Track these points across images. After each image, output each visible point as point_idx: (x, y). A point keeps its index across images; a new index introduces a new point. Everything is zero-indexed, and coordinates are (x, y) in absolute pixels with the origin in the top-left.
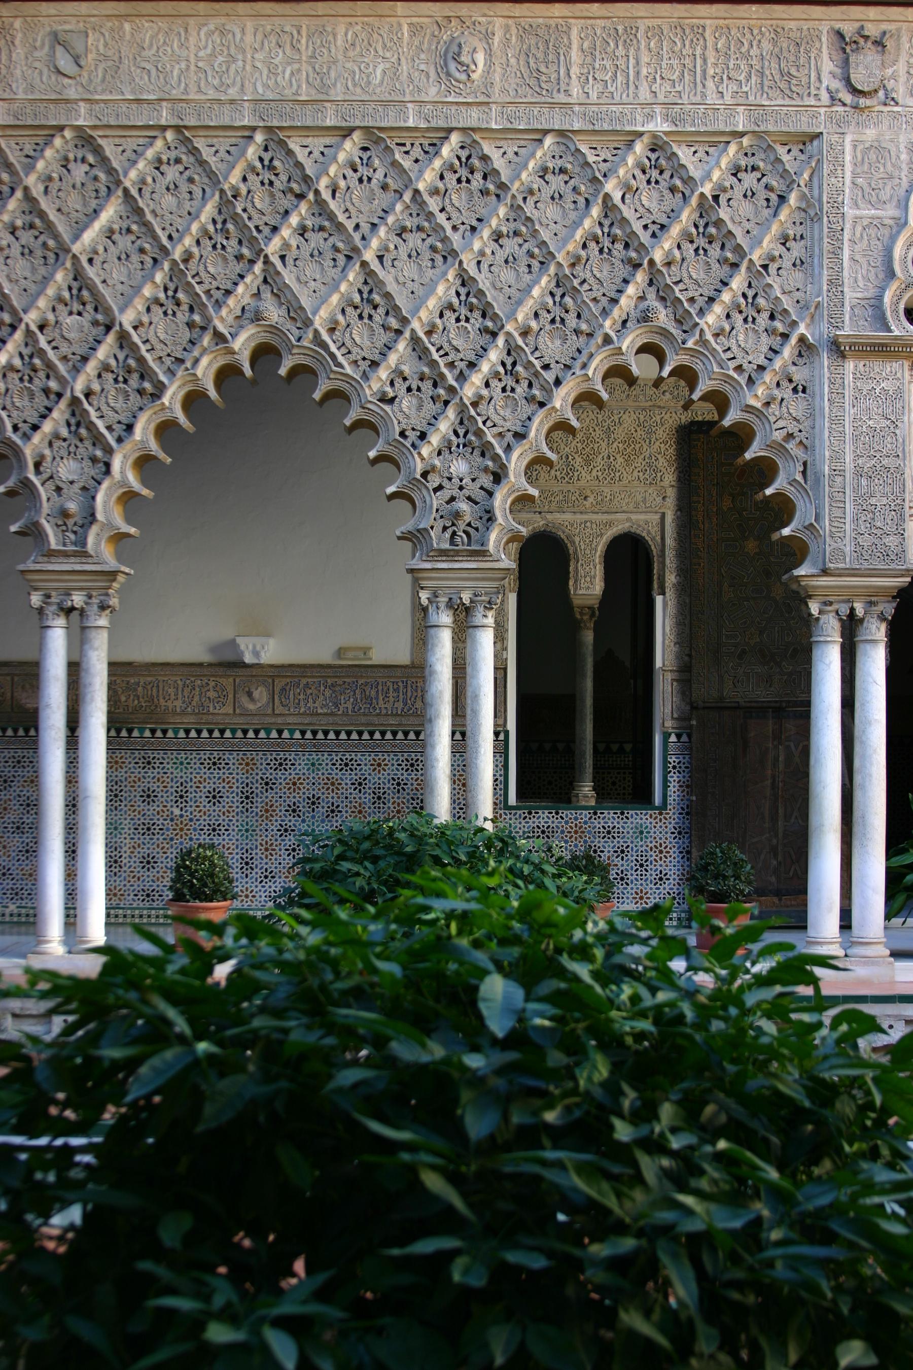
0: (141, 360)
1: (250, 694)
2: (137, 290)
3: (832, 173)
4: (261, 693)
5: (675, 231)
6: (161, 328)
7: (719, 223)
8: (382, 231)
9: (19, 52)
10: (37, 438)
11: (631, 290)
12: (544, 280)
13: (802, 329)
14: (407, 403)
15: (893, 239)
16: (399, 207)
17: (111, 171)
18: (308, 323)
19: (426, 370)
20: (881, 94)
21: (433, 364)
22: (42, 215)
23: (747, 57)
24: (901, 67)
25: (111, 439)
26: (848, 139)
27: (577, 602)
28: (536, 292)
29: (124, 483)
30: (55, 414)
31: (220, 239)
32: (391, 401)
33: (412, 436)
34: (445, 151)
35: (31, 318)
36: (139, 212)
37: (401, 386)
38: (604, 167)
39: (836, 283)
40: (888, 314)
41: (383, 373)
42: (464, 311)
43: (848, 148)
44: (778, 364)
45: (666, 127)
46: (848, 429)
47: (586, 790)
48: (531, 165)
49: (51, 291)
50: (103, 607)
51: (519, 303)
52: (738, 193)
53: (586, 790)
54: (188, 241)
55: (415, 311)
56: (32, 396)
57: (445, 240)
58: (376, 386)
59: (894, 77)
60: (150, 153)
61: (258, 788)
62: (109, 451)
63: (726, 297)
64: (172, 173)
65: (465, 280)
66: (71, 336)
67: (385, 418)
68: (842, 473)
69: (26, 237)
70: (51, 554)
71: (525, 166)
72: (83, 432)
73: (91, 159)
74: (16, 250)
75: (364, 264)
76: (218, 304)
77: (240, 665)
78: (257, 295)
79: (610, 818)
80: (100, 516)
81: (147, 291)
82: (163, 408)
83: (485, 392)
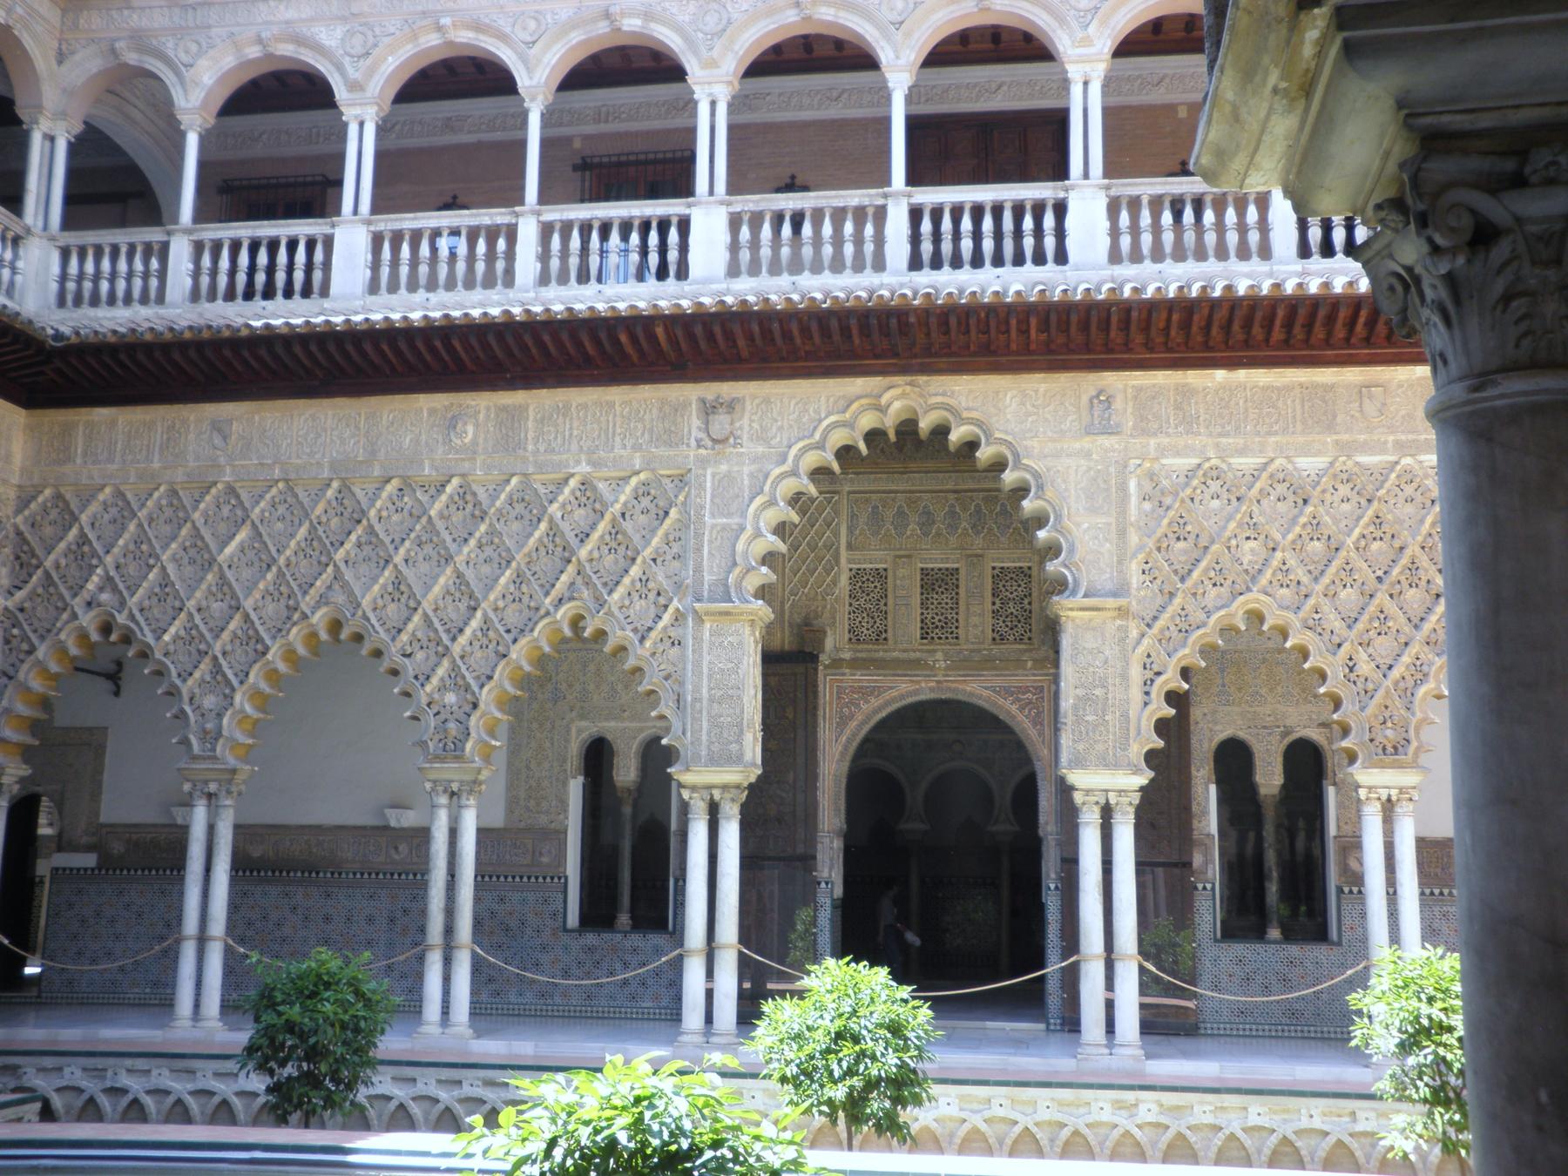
0: (256, 631)
1: (396, 848)
2: (256, 584)
3: (699, 495)
4: (403, 848)
5: (595, 536)
6: (270, 608)
7: (625, 534)
8: (407, 543)
9: (192, 436)
10: (190, 682)
11: (564, 578)
12: (508, 573)
13: (675, 603)
14: (420, 656)
15: (737, 538)
16: (418, 527)
17: (245, 509)
18: (359, 605)
19: (432, 635)
20: (731, 440)
21: (436, 631)
22: (202, 539)
23: (642, 420)
24: (746, 421)
25: (235, 682)
26: (709, 472)
27: (618, 784)
28: (503, 580)
29: (242, 711)
30: (202, 666)
31: (309, 551)
32: (409, 656)
33: (421, 678)
34: (449, 489)
35: (191, 605)
36: (260, 535)
37: (416, 645)
38: (551, 496)
39: (698, 569)
40: (732, 590)
41: (404, 637)
42: (458, 595)
43: (709, 478)
44: (661, 624)
45: (588, 469)
46: (705, 670)
47: (624, 919)
48: (503, 496)
49: (204, 586)
50: (229, 792)
51: (492, 588)
52: (638, 510)
53: (624, 919)
54: (288, 552)
55: (424, 596)
56: (190, 654)
57: (446, 548)
58: (399, 644)
59: (741, 428)
60: (268, 496)
61: (399, 914)
62: (233, 690)
63: (626, 580)
64: (281, 510)
65: (459, 575)
66: (217, 615)
67: (404, 667)
68: (700, 700)
69: (192, 552)
70: (195, 758)
71: (498, 497)
72: (219, 678)
73: (233, 502)
74: (186, 560)
75: (396, 566)
76: (305, 593)
77: (387, 828)
78: (329, 587)
79: (636, 939)
80: (225, 733)
81: (261, 586)
82: (268, 662)
83: (468, 649)
